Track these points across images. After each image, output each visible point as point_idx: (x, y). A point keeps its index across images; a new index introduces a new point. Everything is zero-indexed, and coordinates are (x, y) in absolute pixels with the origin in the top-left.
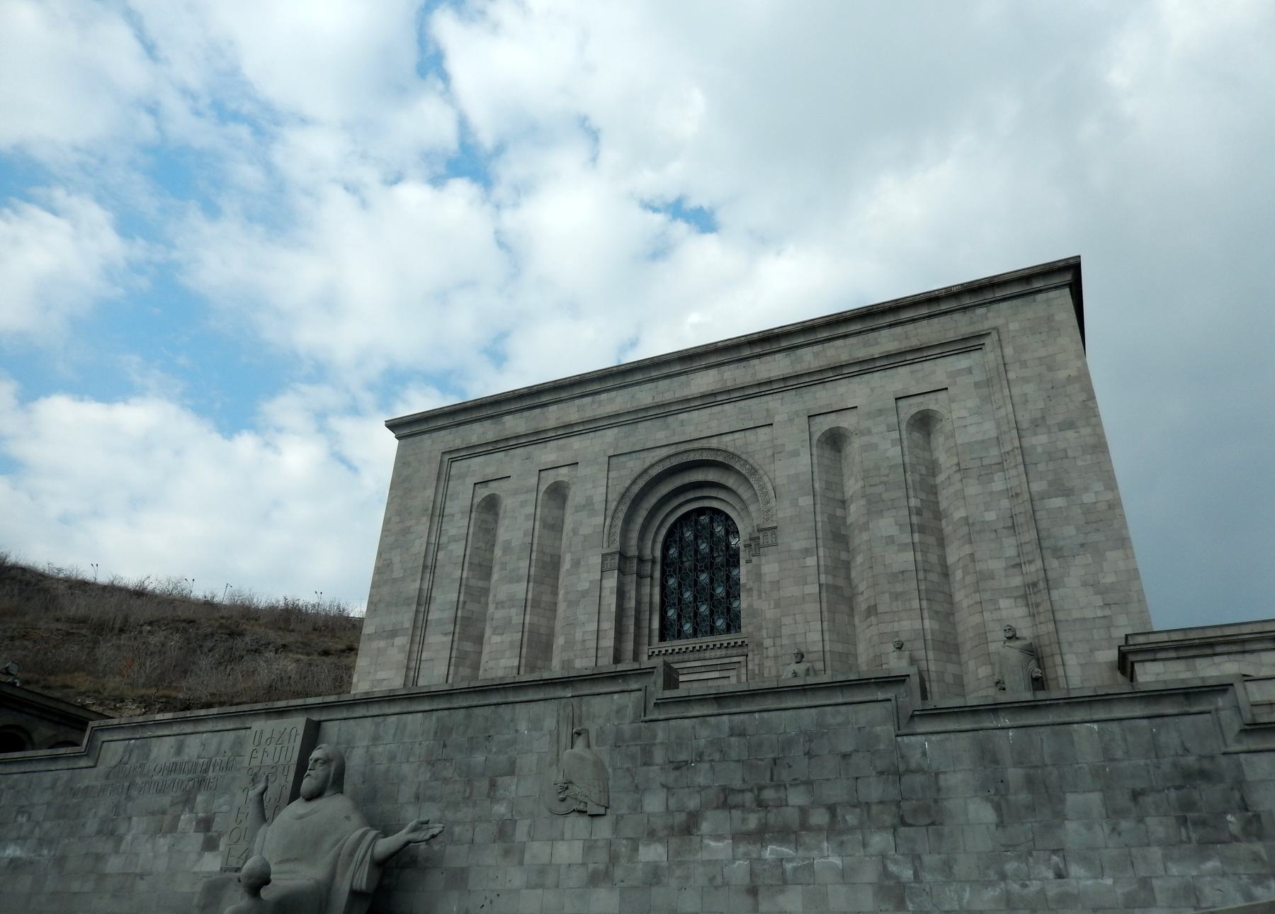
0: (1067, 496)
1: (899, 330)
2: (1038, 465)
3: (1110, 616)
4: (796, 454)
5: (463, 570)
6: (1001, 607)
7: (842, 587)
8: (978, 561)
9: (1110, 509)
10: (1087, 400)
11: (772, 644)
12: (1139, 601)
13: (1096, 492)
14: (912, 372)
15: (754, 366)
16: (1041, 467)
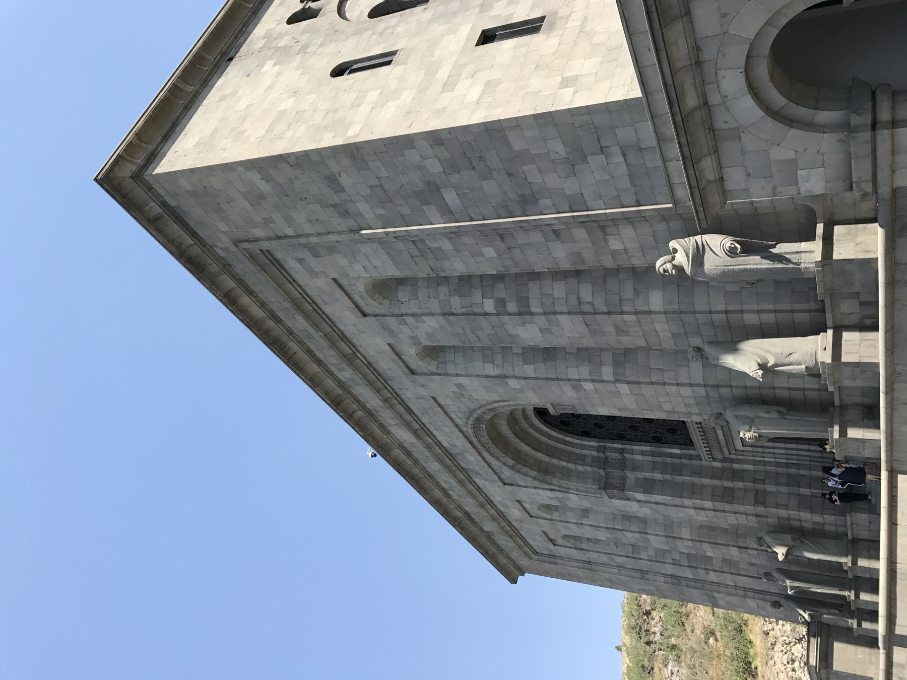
0: (438, 189)
1: (280, 314)
2: (402, 213)
3: (621, 148)
4: (460, 386)
5: (641, 559)
6: (623, 248)
7: (613, 354)
8: (557, 264)
9: (443, 144)
10: (288, 163)
11: (700, 416)
12: (589, 114)
13: (423, 158)
14: (326, 304)
15: (373, 407)
16: (406, 210)
